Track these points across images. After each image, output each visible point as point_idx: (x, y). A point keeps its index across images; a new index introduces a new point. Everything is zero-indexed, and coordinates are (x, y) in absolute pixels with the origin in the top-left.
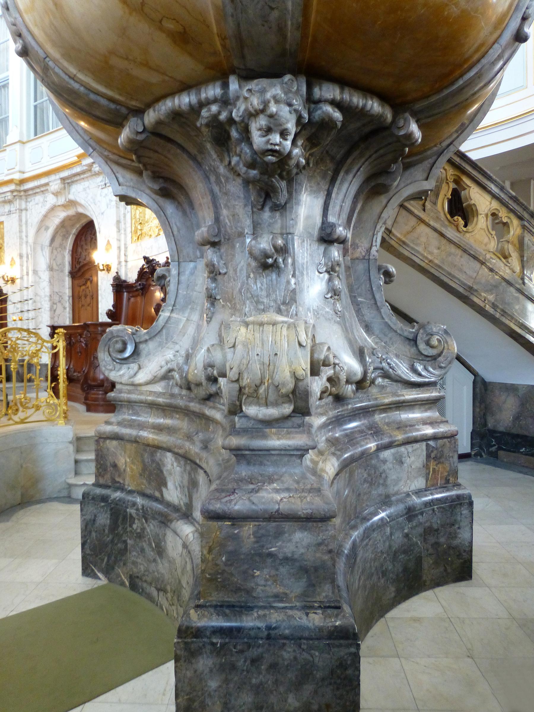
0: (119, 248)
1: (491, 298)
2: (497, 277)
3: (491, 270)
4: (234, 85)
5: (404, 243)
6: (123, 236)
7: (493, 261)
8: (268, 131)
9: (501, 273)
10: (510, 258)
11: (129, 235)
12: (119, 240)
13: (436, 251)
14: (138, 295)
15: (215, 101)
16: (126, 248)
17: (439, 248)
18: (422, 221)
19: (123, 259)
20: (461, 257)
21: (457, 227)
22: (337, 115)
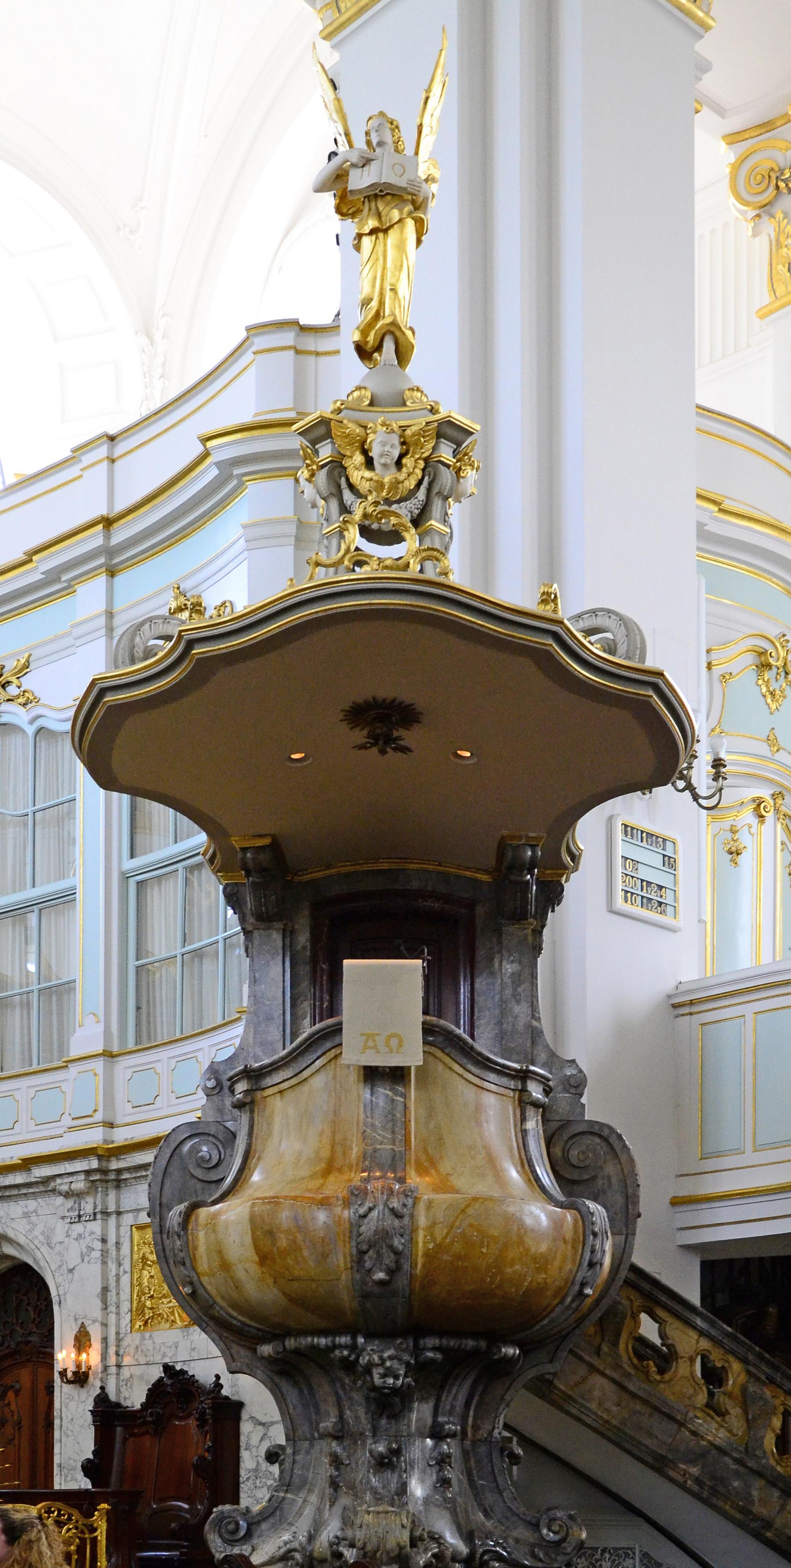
0: (105, 1340)
1: (695, 1470)
2: (704, 1443)
3: (694, 1433)
4: (361, 1340)
5: (570, 1397)
6: (112, 1318)
7: (699, 1421)
8: (384, 1376)
9: (709, 1438)
10: (728, 1416)
11: (126, 1319)
12: (105, 1325)
13: (615, 1409)
14: (146, 1433)
15: (346, 1347)
16: (119, 1340)
17: (618, 1405)
18: (593, 1369)
19: (112, 1360)
20: (650, 1416)
21: (647, 1374)
22: (439, 1356)
